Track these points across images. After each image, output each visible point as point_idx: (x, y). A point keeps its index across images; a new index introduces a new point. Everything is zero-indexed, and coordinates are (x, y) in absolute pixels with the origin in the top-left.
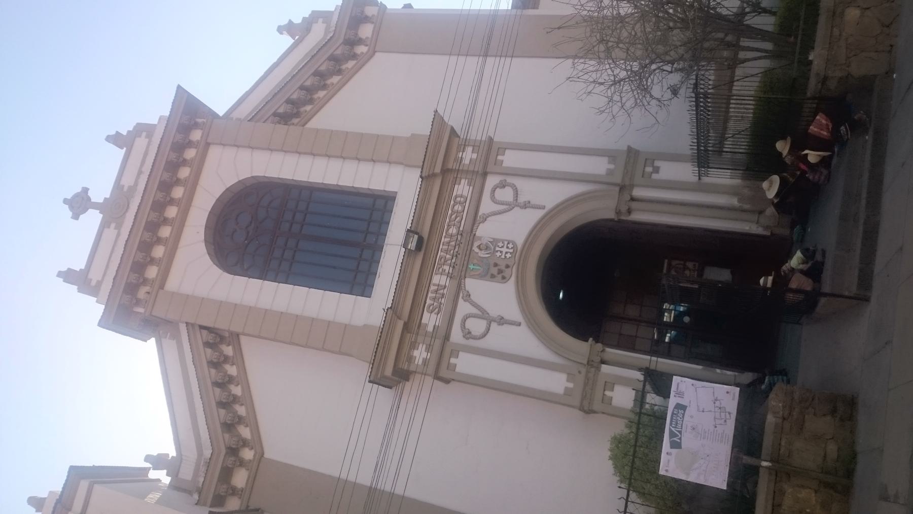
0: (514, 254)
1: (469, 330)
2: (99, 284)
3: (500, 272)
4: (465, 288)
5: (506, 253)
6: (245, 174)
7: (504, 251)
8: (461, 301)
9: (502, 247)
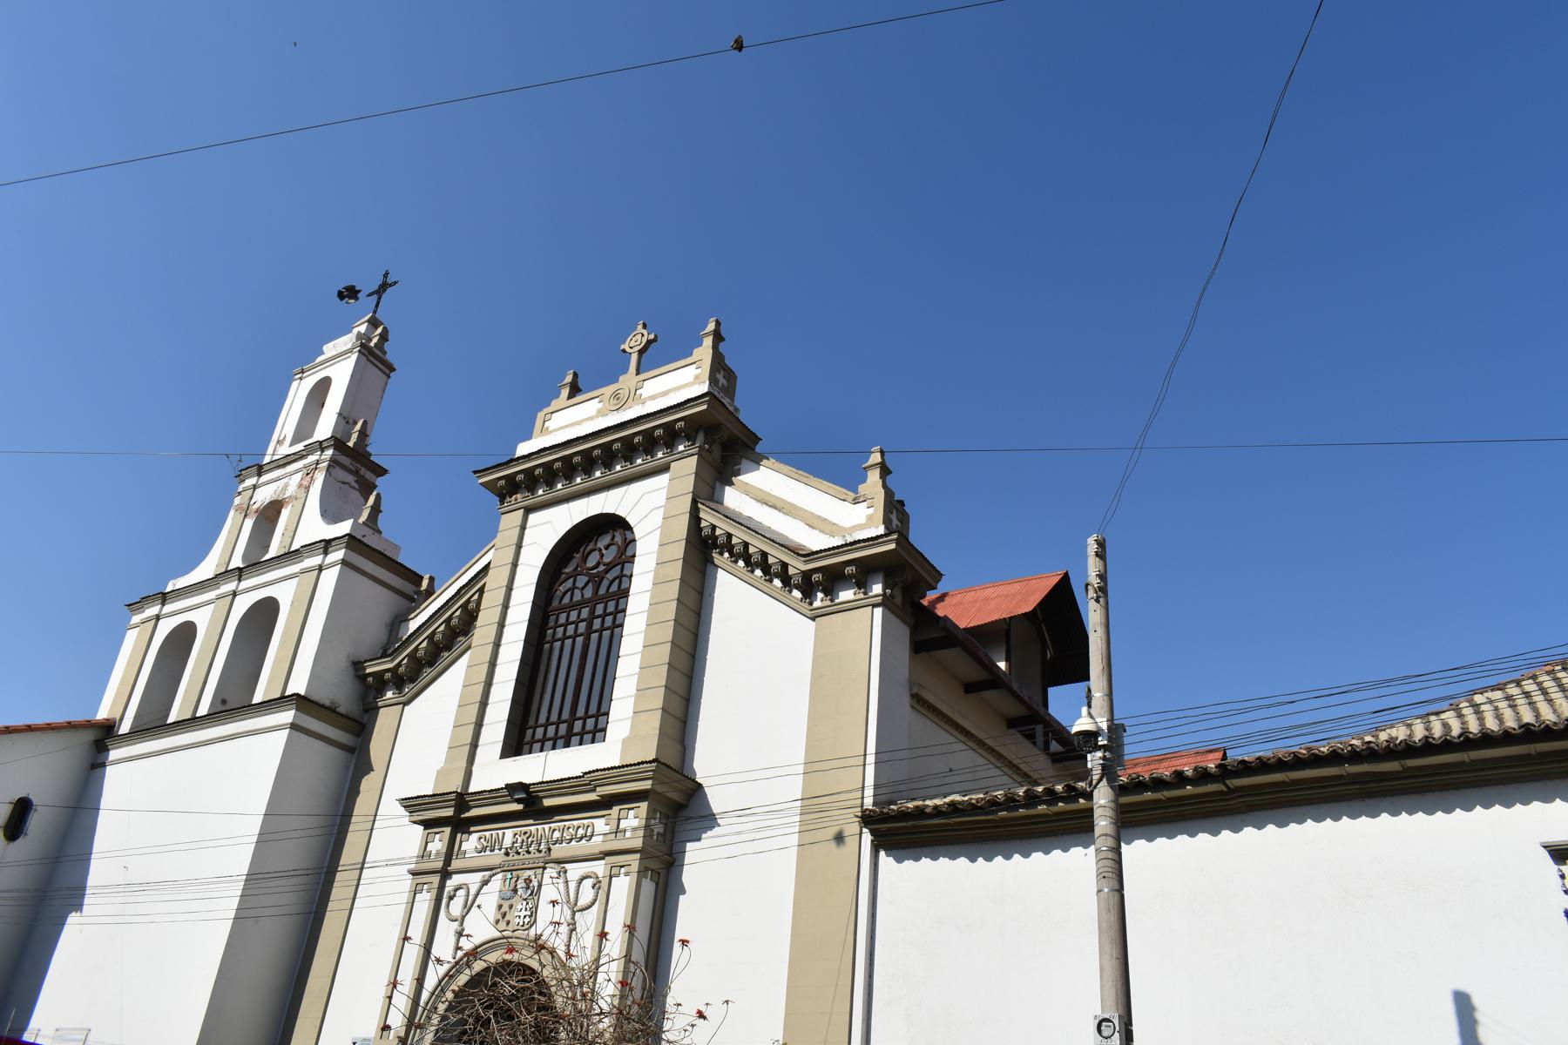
0: (519, 927)
1: (455, 896)
2: (544, 431)
3: (504, 915)
4: (494, 875)
5: (520, 917)
6: (638, 532)
7: (520, 911)
8: (479, 876)
9: (526, 910)
